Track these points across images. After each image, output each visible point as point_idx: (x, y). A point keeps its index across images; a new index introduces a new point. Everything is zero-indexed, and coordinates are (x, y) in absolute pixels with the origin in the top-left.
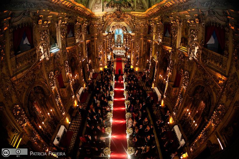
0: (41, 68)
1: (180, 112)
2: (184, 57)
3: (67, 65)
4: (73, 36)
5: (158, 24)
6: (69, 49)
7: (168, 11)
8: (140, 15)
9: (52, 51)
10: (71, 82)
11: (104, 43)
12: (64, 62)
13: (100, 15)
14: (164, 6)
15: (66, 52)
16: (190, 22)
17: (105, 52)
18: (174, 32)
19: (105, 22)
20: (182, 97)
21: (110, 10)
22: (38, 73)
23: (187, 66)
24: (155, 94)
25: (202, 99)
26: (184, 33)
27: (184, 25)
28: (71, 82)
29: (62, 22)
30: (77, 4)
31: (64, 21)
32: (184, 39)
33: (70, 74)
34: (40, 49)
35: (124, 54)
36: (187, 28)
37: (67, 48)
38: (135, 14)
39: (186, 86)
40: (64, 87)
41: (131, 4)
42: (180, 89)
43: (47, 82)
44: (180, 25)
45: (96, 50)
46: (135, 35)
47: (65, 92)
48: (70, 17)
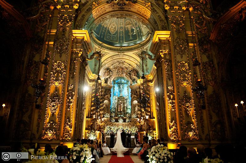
46: (172, 35)
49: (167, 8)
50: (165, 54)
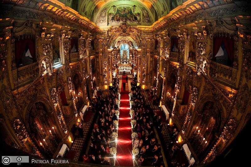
0: (43, 84)
1: (189, 129)
2: (193, 72)
3: (70, 82)
4: (77, 51)
5: (165, 38)
6: (72, 65)
7: (175, 24)
8: (147, 29)
9: (54, 66)
10: (75, 99)
11: (109, 59)
12: (68, 78)
13: (105, 30)
14: (170, 19)
15: (69, 68)
16: (197, 34)
17: (110, 69)
18: (182, 46)
19: (110, 37)
20: (191, 114)
21: (115, 24)
22: (41, 88)
23: (195, 82)
24: (163, 113)
25: (212, 115)
26: (192, 47)
27: (192, 38)
28: (75, 99)
29: (66, 35)
30: (82, 17)
31: (68, 36)
32: (192, 53)
33: (73, 92)
34: (43, 64)
35: (130, 71)
36: (195, 41)
37: (70, 64)
38: (141, 28)
39: (195, 103)
40: (67, 105)
41: (137, 17)
42: (188, 106)
43: (50, 98)
44: (187, 38)
45: (100, 67)
47: (68, 109)
48: (73, 31)
49: (141, 40)
50: (139, 57)
